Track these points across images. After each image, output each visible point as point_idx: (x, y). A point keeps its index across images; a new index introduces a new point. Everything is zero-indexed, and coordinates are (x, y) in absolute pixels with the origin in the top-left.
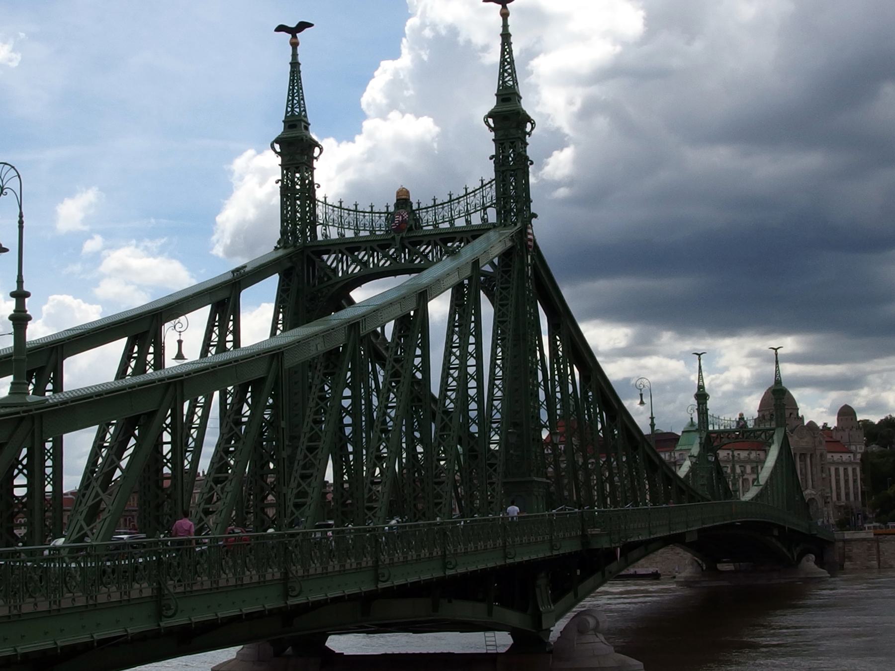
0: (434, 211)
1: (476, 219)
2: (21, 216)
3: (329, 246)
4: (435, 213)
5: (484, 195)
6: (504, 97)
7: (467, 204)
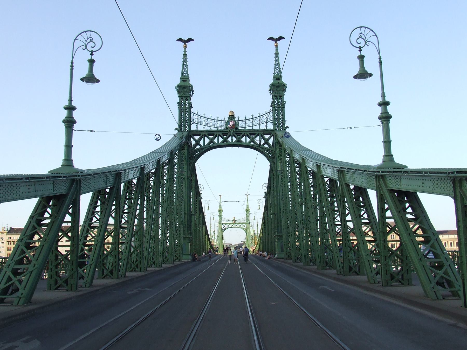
0: (245, 122)
1: (263, 127)
2: (380, 58)
3: (197, 133)
4: (246, 123)
6: (276, 78)
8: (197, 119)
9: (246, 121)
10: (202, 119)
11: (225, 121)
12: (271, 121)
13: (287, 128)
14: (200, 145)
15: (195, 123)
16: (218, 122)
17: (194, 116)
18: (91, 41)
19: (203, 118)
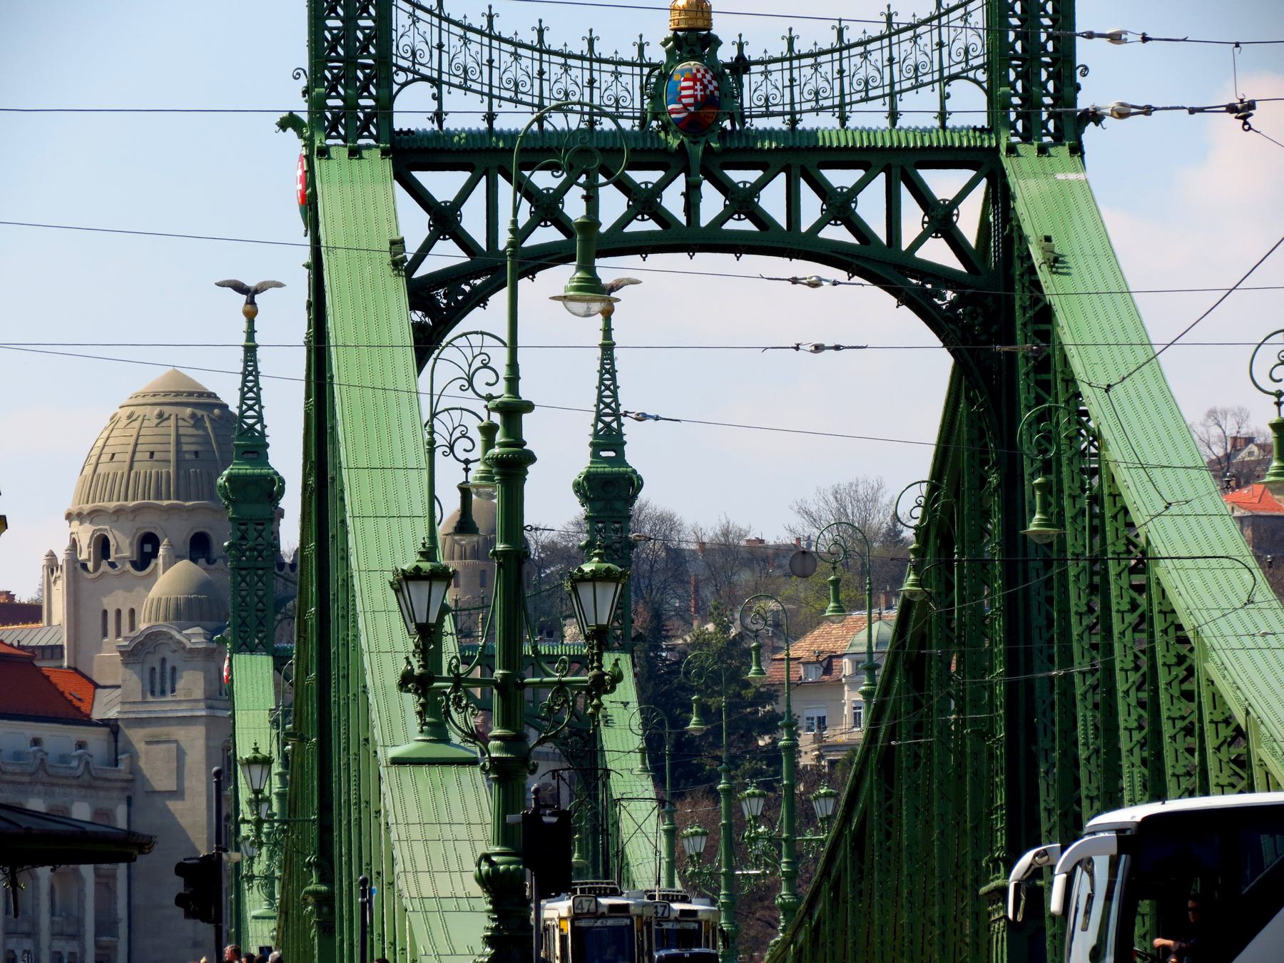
0: (787, 74)
4: (792, 80)
5: (945, 39)
7: (891, 60)
8: (436, 52)
9: (791, 69)
10: (474, 47)
11: (641, 66)
12: (978, 68)
13: (1092, 124)
14: (465, 242)
15: (424, 78)
16: (591, 70)
17: (420, 25)
18: (485, 366)
19: (486, 40)
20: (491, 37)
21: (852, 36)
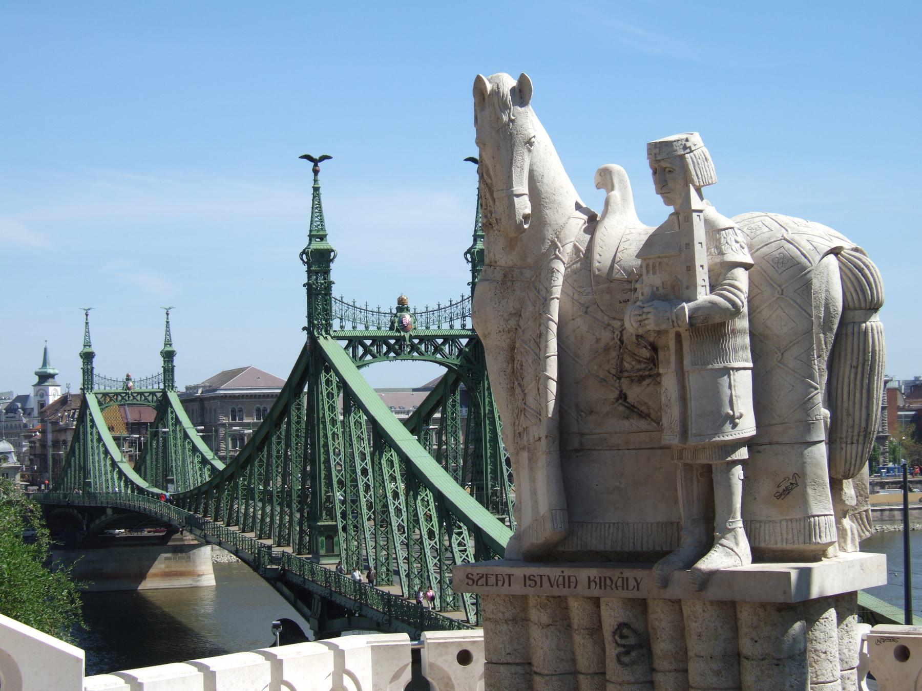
20: (355, 307)
21: (442, 306)
